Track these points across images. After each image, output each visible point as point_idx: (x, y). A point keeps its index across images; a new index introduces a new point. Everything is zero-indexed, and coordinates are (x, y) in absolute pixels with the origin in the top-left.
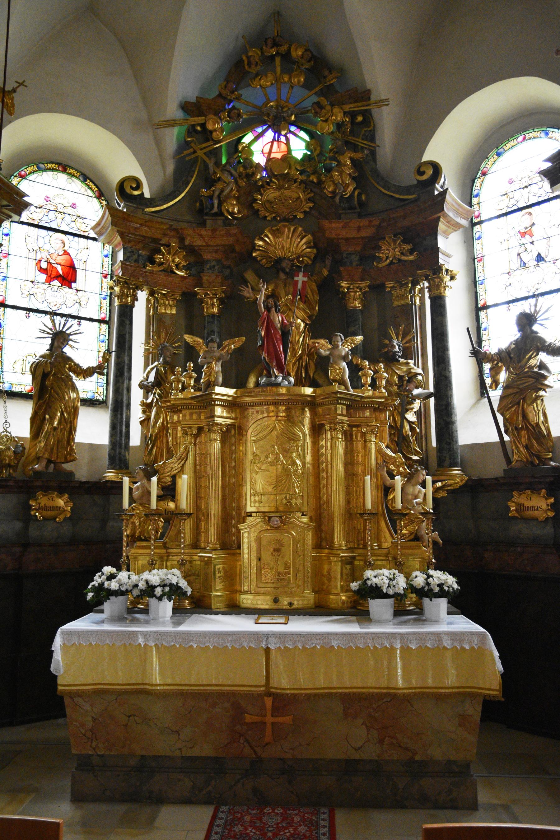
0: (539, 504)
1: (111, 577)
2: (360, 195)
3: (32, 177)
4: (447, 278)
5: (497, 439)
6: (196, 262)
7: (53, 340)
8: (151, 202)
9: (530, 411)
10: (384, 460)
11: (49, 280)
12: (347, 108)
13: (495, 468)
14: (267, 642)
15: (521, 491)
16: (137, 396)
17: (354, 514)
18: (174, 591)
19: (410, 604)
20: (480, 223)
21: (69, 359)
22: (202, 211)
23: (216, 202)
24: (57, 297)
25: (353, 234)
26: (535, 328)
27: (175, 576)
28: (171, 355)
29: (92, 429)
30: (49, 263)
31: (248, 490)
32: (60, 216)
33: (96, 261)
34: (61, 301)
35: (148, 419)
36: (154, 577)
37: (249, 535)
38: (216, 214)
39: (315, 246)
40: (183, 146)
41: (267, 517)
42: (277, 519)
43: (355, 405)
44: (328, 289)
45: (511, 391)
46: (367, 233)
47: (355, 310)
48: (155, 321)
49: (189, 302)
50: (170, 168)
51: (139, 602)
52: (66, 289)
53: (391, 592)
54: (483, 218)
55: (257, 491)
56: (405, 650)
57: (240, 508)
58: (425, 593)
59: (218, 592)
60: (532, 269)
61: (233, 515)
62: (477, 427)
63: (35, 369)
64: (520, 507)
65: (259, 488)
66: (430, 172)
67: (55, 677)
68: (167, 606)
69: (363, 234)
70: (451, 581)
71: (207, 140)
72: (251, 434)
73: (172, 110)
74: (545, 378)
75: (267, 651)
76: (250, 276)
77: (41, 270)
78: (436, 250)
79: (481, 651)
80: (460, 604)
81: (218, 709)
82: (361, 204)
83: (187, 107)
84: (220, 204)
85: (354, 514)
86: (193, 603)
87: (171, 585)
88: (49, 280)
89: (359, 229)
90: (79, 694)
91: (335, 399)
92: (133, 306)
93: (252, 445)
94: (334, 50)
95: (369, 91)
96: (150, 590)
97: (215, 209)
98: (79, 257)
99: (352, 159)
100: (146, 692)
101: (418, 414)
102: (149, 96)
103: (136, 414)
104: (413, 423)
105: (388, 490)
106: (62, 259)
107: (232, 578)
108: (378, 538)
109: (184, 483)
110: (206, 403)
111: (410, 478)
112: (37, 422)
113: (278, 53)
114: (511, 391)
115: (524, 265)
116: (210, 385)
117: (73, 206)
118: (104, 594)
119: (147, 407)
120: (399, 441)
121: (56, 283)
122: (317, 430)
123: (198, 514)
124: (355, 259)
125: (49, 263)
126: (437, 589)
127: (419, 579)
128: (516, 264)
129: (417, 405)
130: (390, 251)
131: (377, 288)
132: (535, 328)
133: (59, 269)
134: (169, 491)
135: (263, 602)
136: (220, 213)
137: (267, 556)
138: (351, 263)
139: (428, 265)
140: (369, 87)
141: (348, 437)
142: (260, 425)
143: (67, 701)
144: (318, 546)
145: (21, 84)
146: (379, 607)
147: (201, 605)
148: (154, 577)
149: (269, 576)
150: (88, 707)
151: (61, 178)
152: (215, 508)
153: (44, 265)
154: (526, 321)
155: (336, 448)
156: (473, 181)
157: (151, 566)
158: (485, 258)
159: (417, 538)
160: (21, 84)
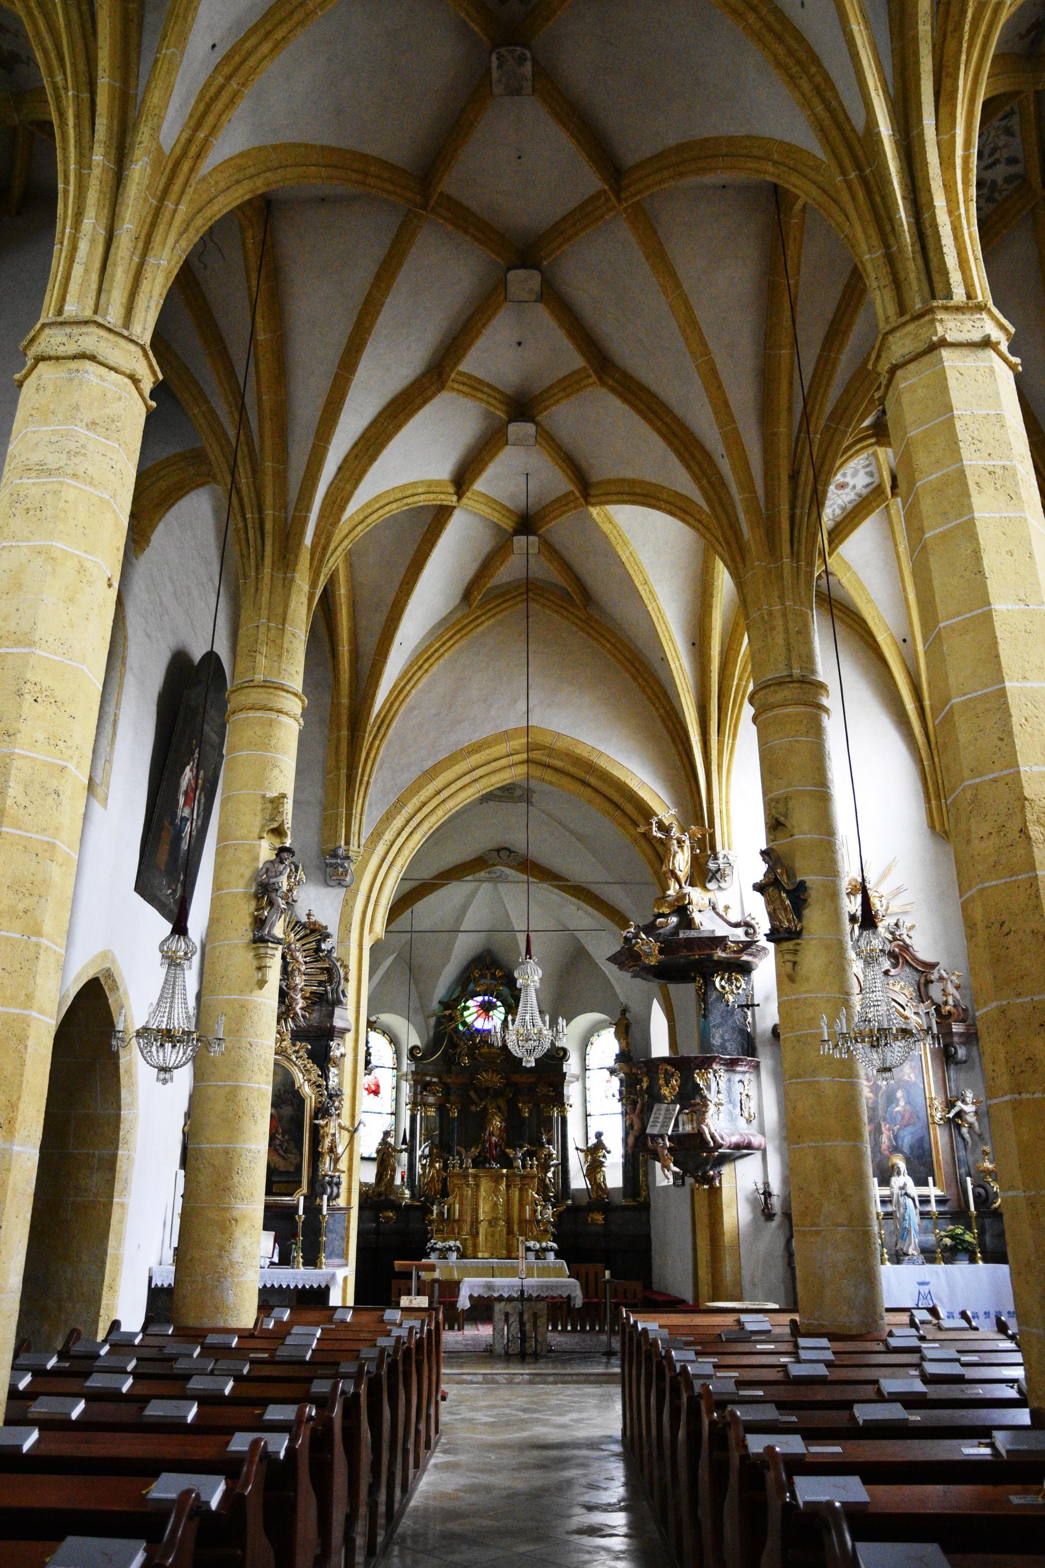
0: (599, 1218)
4: (568, 1108)
6: (447, 1089)
9: (598, 1176)
10: (535, 1200)
11: (369, 1093)
13: (584, 1201)
15: (593, 1212)
17: (522, 1221)
18: (458, 1249)
19: (540, 1254)
22: (449, 1061)
27: (458, 1243)
28: (442, 1148)
31: (481, 1210)
35: (424, 1172)
36: (452, 1243)
37: (482, 1229)
39: (506, 1079)
40: (439, 1023)
41: (490, 1222)
42: (493, 1222)
43: (523, 1177)
44: (512, 1104)
46: (532, 1080)
47: (525, 1118)
48: (426, 1119)
49: (441, 1109)
50: (431, 1033)
51: (444, 1253)
55: (484, 1211)
56: (538, 1268)
57: (477, 1218)
58: (545, 1250)
59: (470, 1251)
61: (475, 1222)
62: (578, 1182)
64: (592, 1219)
65: (486, 1209)
66: (562, 1054)
68: (455, 1255)
70: (555, 1245)
73: (435, 1005)
76: (472, 1094)
78: (563, 1094)
79: (562, 1267)
80: (558, 1255)
85: (522, 1221)
86: (462, 1256)
88: (369, 1093)
91: (516, 1176)
93: (483, 1193)
96: (450, 1249)
101: (554, 1173)
102: (423, 998)
105: (536, 1211)
106: (374, 1081)
107: (475, 1246)
108: (531, 1231)
110: (466, 1176)
111: (544, 1207)
112: (379, 1176)
116: (467, 1168)
118: (433, 1249)
119: (424, 1166)
120: (543, 1189)
122: (508, 1186)
127: (544, 1244)
129: (552, 1169)
130: (541, 1090)
131: (537, 1106)
135: (486, 1255)
136: (459, 1063)
137: (489, 1238)
139: (559, 1100)
141: (521, 1190)
142: (485, 1185)
144: (508, 1234)
148: (452, 1243)
149: (489, 1245)
154: (599, 1135)
155: (516, 1194)
157: (444, 1240)
159: (546, 1231)
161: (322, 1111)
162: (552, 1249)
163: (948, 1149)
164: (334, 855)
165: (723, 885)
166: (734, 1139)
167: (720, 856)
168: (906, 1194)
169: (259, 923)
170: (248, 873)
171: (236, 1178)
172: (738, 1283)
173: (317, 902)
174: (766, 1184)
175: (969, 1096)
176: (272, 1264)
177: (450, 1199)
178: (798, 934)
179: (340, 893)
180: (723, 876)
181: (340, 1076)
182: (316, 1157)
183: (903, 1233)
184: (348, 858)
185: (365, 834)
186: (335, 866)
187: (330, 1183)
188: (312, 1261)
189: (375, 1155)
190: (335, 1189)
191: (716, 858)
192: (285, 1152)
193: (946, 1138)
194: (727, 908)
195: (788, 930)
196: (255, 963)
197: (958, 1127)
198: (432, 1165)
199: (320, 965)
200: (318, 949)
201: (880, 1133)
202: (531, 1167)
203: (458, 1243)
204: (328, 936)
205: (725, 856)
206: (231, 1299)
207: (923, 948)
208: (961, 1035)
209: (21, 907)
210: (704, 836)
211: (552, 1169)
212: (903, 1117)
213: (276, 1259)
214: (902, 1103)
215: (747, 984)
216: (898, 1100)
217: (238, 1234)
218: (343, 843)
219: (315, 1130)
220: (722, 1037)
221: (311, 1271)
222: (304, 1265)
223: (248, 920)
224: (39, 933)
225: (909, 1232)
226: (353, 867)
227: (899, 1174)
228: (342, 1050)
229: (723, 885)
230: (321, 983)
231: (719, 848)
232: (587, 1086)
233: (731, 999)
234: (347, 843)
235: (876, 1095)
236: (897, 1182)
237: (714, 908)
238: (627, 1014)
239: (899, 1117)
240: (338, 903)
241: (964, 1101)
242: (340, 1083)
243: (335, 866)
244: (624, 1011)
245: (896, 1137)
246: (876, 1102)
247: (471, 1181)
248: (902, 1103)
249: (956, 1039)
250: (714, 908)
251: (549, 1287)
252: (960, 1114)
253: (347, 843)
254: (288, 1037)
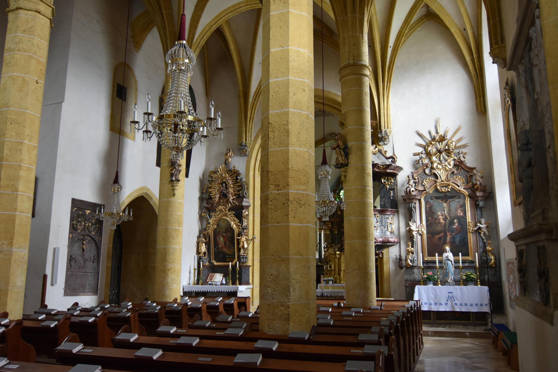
16: (323, 249)
18: (332, 280)
27: (332, 278)
36: (330, 278)
49: (331, 231)
51: (327, 282)
61: (340, 270)
72: (342, 259)
96: (329, 280)
103: (323, 253)
109: (333, 265)
110: (335, 254)
119: (325, 251)
123: (335, 270)
134: (330, 267)
147: (336, 283)
148: (330, 278)
152: (337, 269)
161: (240, 234)
163: (476, 242)
164: (241, 145)
165: (386, 143)
166: (381, 239)
167: (383, 132)
168: (448, 260)
169: (172, 175)
170: (168, 159)
171: (168, 257)
172: (389, 292)
173: (237, 163)
174: (400, 256)
175: (483, 221)
176: (222, 284)
177: (331, 263)
178: (347, 165)
179: (246, 158)
180: (385, 139)
181: (248, 222)
182: (239, 250)
183: (446, 274)
184: (246, 146)
185: (253, 136)
186: (242, 149)
187: (243, 258)
188: (234, 283)
190: (245, 260)
191: (381, 133)
192: (230, 247)
193: (475, 238)
194: (386, 152)
195: (342, 164)
196: (172, 188)
197: (480, 233)
198: (327, 251)
199: (238, 184)
200: (237, 179)
201: (447, 236)
203: (332, 278)
204: (240, 174)
205: (385, 131)
206: (168, 293)
207: (469, 162)
208: (482, 197)
209: (11, 184)
210: (377, 124)
212: (457, 230)
213: (225, 283)
214: (456, 224)
215: (394, 180)
216: (455, 223)
217: (169, 274)
218: (244, 141)
219: (238, 240)
220: (384, 201)
221: (234, 286)
222: (232, 284)
223: (169, 174)
224: (17, 191)
225: (449, 273)
226: (249, 149)
227: (446, 252)
228: (247, 213)
229: (386, 143)
230: (238, 191)
231: (383, 128)
233: (388, 187)
234: (246, 140)
235: (445, 221)
236: (445, 255)
237: (381, 153)
239: (455, 230)
240: (245, 162)
241: (481, 223)
242: (248, 224)
243: (242, 149)
245: (453, 238)
246: (445, 224)
247: (338, 256)
248: (456, 224)
249: (480, 198)
250: (381, 153)
251: (335, 293)
252: (480, 228)
253: (246, 140)
254: (227, 210)
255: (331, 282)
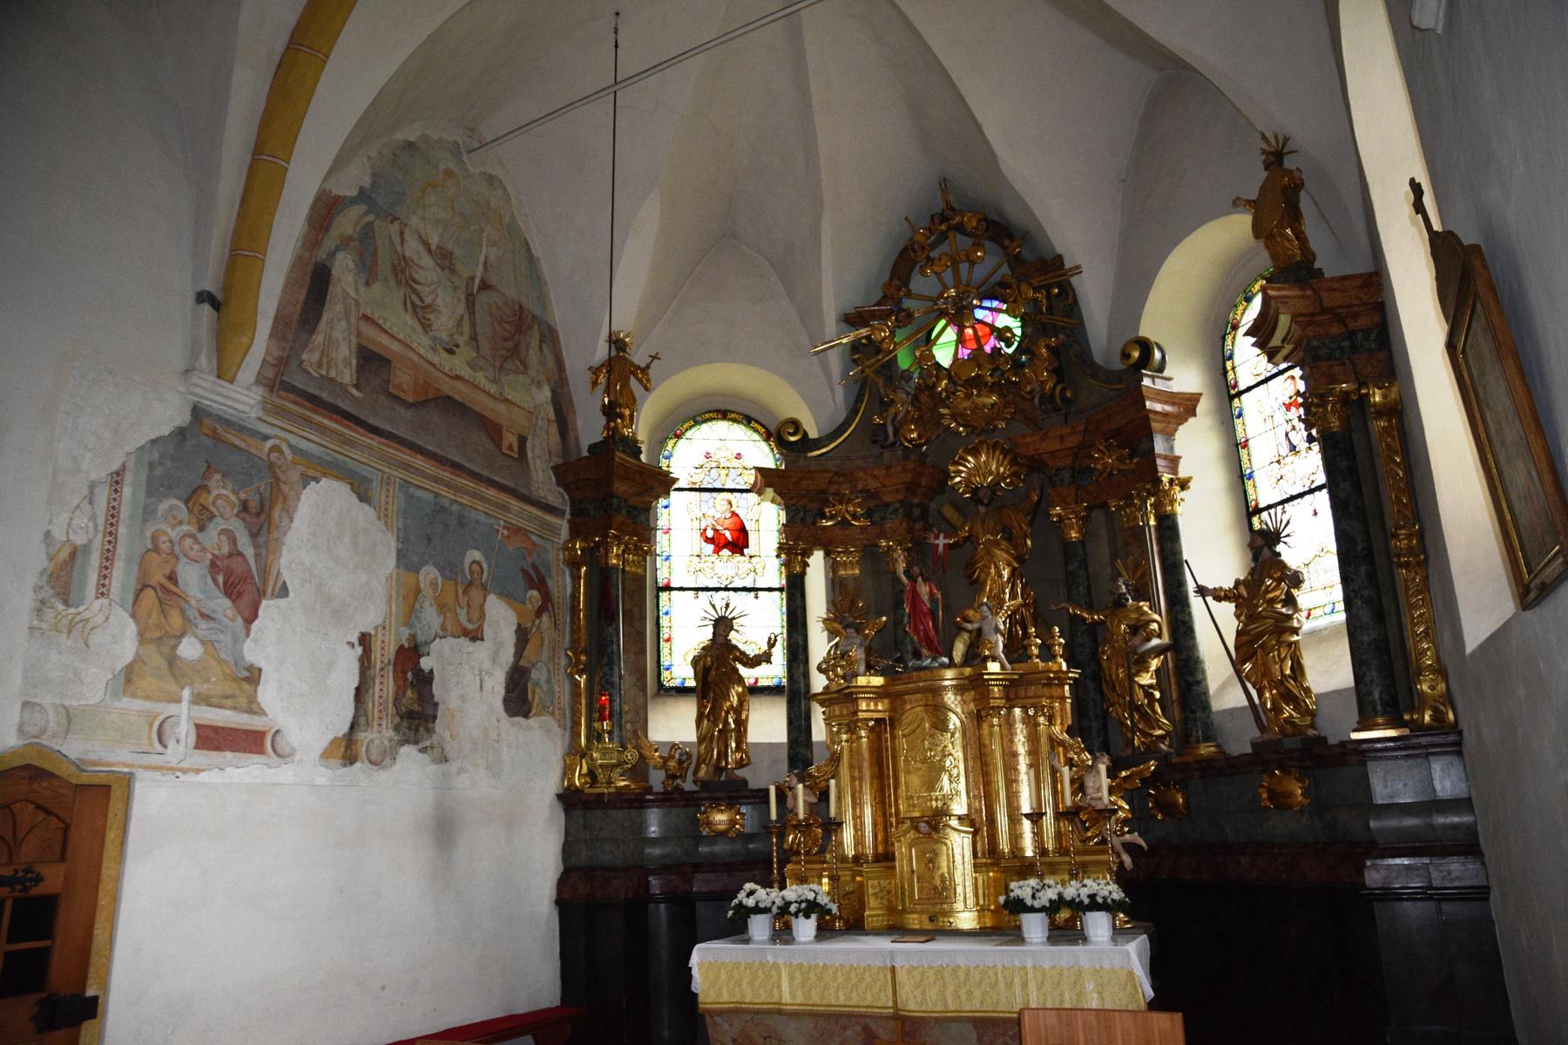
1: (751, 893)
2: (1063, 390)
3: (689, 434)
5: (1246, 703)
6: (876, 509)
7: (715, 627)
8: (817, 444)
12: (1035, 282)
14: (892, 959)
20: (1239, 394)
21: (736, 648)
23: (890, 430)
24: (728, 567)
25: (1052, 445)
26: (1279, 548)
29: (767, 725)
30: (716, 530)
32: (724, 472)
33: (766, 520)
34: (732, 573)
38: (893, 444)
45: (1244, 638)
48: (836, 586)
49: (872, 557)
52: (738, 557)
53: (1037, 904)
54: (1242, 387)
59: (874, 912)
60: (1303, 453)
63: (695, 662)
67: (695, 995)
69: (1068, 444)
71: (878, 351)
74: (1290, 617)
75: (893, 969)
77: (708, 540)
81: (849, 1032)
82: (1067, 402)
83: (852, 319)
84: (896, 431)
87: (807, 901)
88: (717, 551)
89: (1062, 438)
90: (720, 1013)
92: (803, 574)
94: (1013, 213)
95: (1060, 258)
97: (891, 438)
98: (749, 516)
99: (1047, 347)
100: (780, 1012)
104: (1151, 686)
113: (949, 228)
114: (1244, 638)
115: (1293, 448)
117: (738, 456)
118: (745, 913)
121: (726, 552)
124: (1066, 474)
125: (716, 530)
126: (1086, 901)
128: (1285, 450)
129: (1155, 664)
132: (1279, 548)
133: (728, 535)
138: (1062, 481)
140: (1059, 250)
143: (708, 1019)
145: (654, 357)
146: (1034, 926)
148: (792, 892)
150: (726, 1027)
151: (721, 428)
153: (710, 534)
156: (1224, 339)
158: (1251, 443)
160: (654, 357)
162: (1094, 905)
189: (691, 683)
202: (1047, 653)
211: (1155, 664)
232: (1240, 436)
238: (1289, 163)
244: (1275, 158)
255: (805, 928)
